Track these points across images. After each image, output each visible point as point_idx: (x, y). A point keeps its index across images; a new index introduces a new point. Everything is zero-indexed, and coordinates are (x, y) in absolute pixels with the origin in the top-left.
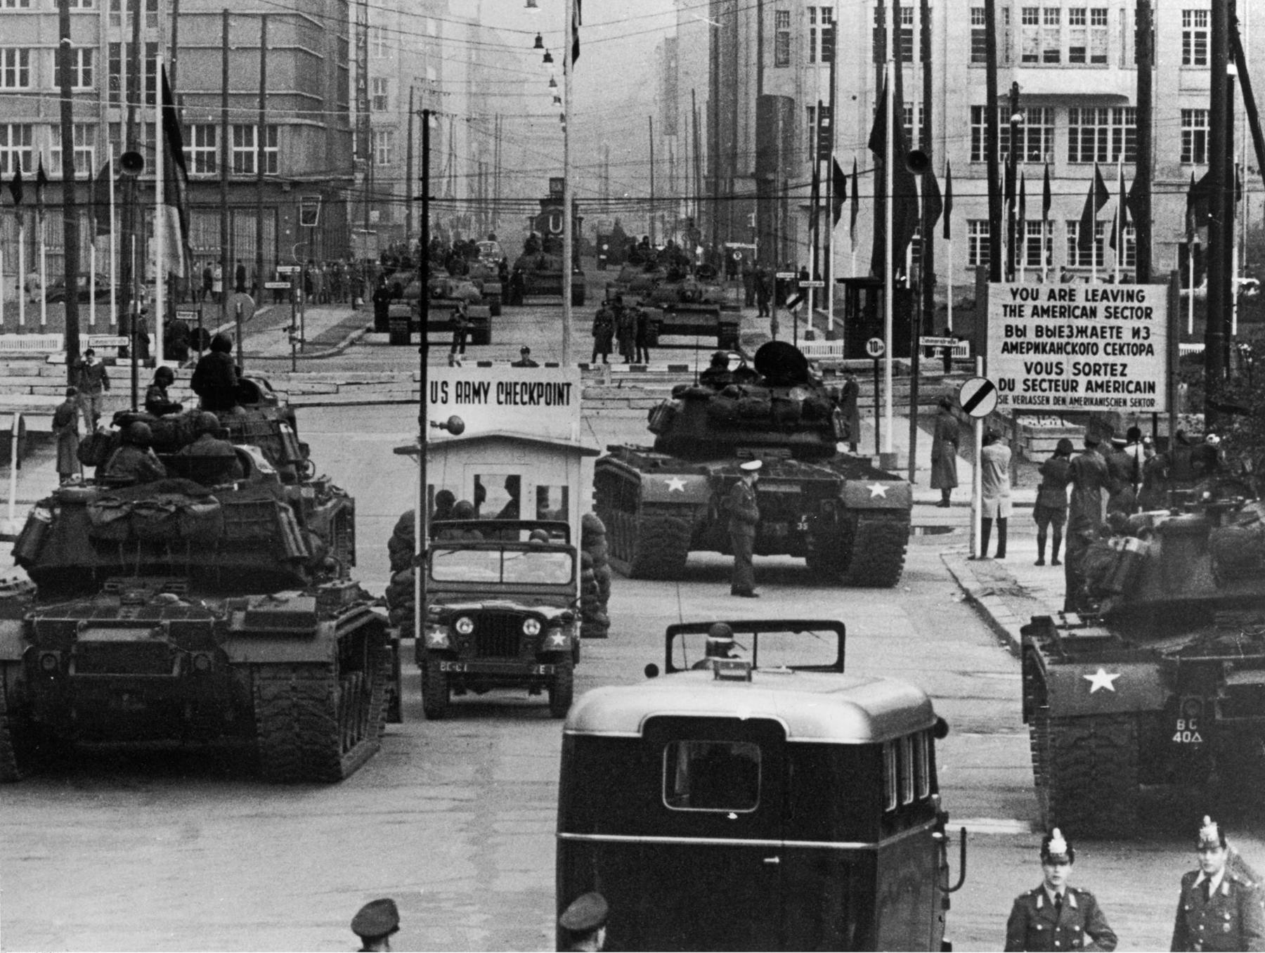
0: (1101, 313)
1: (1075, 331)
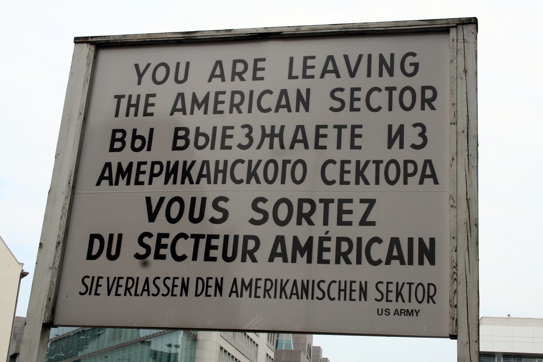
0: (320, 101)
1: (257, 135)
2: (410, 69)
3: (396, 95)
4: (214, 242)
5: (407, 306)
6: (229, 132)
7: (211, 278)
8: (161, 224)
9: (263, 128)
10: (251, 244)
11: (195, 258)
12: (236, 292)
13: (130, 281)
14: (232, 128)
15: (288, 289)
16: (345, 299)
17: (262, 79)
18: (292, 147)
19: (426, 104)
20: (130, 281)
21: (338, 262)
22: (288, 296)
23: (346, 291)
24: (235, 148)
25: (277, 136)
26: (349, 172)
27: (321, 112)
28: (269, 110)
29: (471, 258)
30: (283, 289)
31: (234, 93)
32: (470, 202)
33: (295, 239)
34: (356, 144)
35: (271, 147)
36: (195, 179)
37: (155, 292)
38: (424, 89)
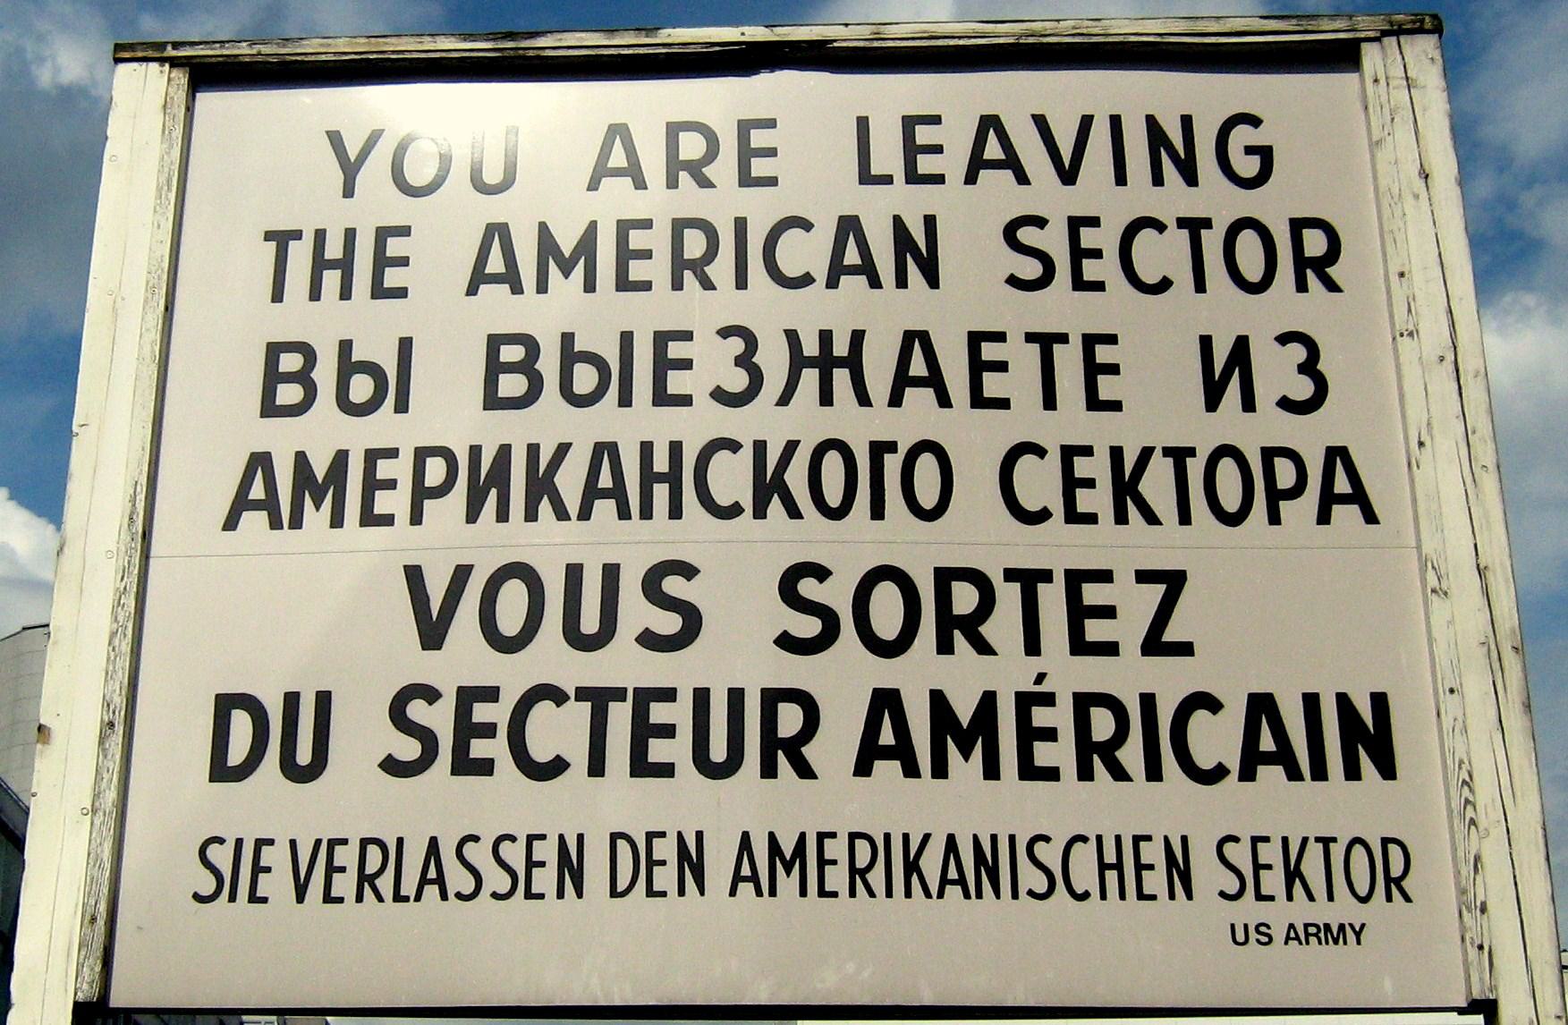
1: (773, 359)
2: (1248, 167)
3: (1212, 242)
4: (659, 713)
5: (1323, 912)
6: (675, 350)
7: (662, 835)
8: (465, 657)
9: (792, 337)
10: (790, 719)
11: (597, 767)
12: (754, 878)
13: (374, 854)
14: (687, 336)
15: (931, 864)
16: (1122, 896)
17: (772, 182)
18: (896, 400)
19: (1310, 274)
20: (374, 854)
21: (1085, 773)
22: (934, 890)
23: (1121, 867)
24: (702, 400)
25: (841, 363)
26: (1090, 483)
27: (974, 290)
28: (806, 280)
29: (1513, 753)
30: (912, 867)
31: (679, 226)
32: (1490, 575)
33: (938, 701)
34: (1104, 394)
35: (826, 398)
36: (573, 506)
37: (469, 887)
38: (1298, 226)
